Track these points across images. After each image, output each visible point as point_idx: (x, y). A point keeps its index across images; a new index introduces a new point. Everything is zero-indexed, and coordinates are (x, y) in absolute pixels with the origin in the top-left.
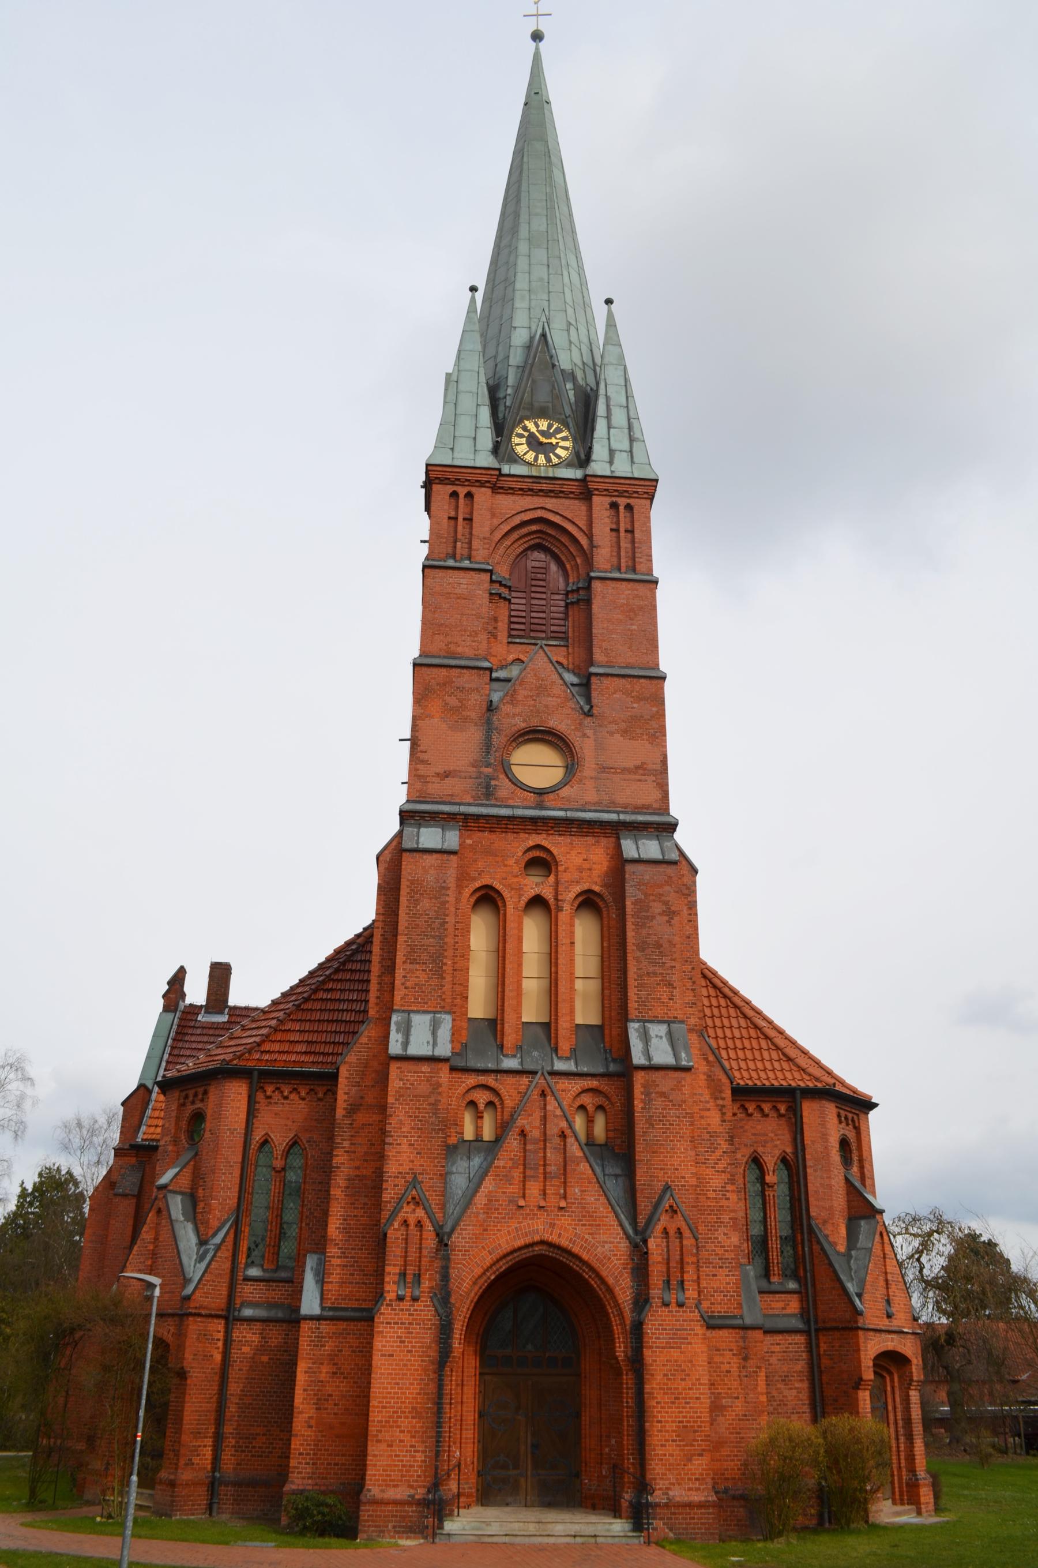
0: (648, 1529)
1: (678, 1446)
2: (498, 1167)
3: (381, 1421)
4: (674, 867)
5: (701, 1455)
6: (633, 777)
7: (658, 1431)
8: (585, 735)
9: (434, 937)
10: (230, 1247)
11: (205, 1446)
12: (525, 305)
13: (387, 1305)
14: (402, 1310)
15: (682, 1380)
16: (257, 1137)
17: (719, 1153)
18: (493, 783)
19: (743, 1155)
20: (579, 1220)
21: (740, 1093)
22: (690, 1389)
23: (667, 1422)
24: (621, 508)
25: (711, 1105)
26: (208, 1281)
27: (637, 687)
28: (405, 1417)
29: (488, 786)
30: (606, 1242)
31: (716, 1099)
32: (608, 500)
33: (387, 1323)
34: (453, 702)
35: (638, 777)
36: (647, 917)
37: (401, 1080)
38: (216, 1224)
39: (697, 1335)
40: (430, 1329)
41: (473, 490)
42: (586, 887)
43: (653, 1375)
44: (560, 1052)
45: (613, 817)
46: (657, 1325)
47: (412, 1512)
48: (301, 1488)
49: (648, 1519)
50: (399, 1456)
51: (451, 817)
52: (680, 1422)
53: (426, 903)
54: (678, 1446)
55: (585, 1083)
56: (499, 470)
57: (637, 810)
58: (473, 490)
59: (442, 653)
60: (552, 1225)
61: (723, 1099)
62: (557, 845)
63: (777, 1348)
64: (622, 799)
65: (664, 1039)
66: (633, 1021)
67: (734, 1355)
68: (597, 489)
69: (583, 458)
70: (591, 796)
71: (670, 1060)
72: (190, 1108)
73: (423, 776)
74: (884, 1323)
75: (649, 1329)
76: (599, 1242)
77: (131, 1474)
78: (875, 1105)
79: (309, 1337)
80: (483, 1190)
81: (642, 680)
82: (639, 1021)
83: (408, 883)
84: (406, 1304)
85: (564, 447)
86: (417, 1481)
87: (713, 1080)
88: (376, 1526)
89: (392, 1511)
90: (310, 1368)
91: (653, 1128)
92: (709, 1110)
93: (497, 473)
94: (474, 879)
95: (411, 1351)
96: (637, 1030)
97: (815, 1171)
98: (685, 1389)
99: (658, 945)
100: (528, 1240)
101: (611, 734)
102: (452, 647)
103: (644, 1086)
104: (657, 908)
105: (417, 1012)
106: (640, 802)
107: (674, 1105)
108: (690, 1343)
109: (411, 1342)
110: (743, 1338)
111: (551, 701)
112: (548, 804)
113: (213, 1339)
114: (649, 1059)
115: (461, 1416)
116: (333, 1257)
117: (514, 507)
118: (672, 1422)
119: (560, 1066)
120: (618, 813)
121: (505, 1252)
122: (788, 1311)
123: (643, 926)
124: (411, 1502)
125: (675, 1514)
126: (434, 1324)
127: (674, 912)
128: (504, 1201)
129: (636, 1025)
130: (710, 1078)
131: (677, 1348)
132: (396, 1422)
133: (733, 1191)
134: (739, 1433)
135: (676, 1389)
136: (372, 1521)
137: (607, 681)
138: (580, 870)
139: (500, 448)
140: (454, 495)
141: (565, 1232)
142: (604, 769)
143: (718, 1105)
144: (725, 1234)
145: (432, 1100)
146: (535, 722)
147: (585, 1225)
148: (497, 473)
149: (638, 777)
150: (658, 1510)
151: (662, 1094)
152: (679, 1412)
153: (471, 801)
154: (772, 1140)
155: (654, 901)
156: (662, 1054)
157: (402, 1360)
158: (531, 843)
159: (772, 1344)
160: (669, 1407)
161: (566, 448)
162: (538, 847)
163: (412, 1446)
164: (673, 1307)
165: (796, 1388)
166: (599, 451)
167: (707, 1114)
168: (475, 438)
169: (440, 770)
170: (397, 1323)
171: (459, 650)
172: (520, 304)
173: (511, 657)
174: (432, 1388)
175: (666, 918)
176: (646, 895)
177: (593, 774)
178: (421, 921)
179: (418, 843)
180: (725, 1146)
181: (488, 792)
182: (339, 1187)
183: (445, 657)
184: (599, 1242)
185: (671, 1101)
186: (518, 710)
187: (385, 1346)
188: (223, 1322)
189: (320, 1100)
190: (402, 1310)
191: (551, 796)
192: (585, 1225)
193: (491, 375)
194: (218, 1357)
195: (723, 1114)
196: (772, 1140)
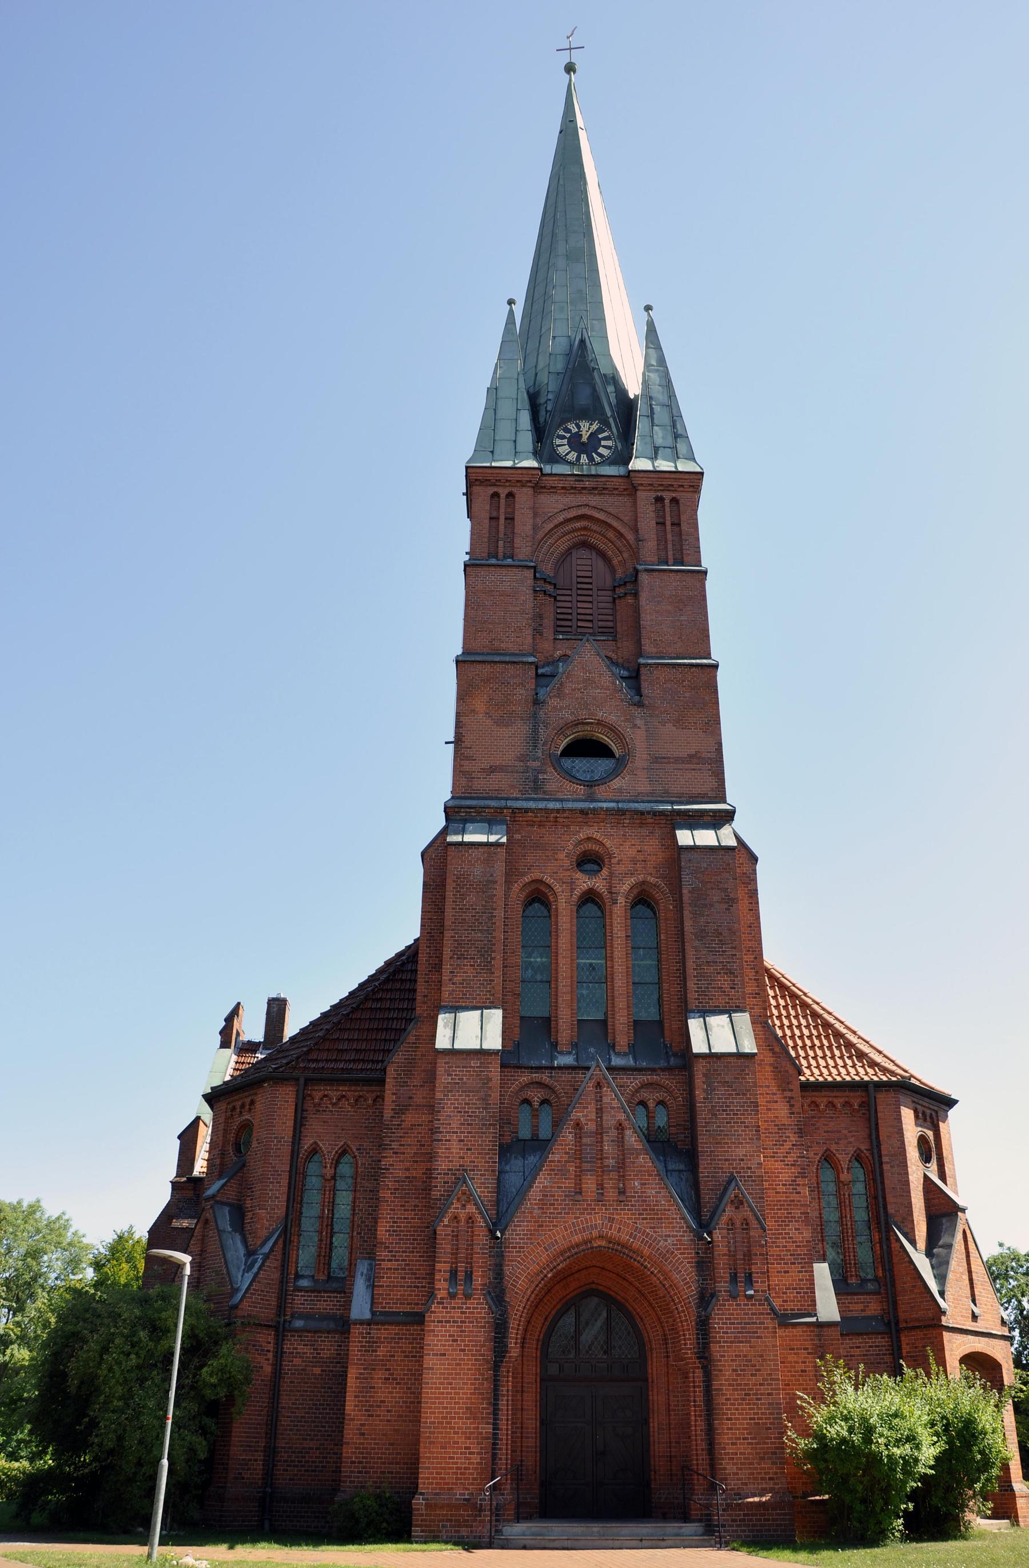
1: (749, 1444)
2: (553, 1161)
3: (434, 1423)
7: (728, 1429)
8: (635, 726)
10: (279, 1257)
11: (256, 1460)
13: (438, 1303)
14: (454, 1308)
15: (752, 1375)
17: (788, 1145)
19: (815, 1154)
22: (761, 1384)
23: (738, 1419)
24: (667, 502)
28: (461, 1418)
29: (536, 780)
30: (669, 1236)
31: (784, 1090)
32: (654, 495)
33: (438, 1322)
38: (264, 1233)
39: (767, 1328)
40: (484, 1327)
41: (514, 490)
43: (721, 1370)
46: (725, 1318)
50: (453, 1458)
52: (751, 1419)
53: (472, 898)
54: (749, 1444)
56: (541, 469)
61: (791, 1090)
67: (809, 1353)
70: (643, 787)
74: (970, 1325)
76: (661, 1236)
78: (955, 1102)
79: (359, 1342)
90: (361, 1374)
91: (717, 1118)
94: (523, 874)
95: (464, 1350)
97: (892, 1167)
101: (663, 723)
102: (496, 643)
109: (464, 1341)
110: (818, 1336)
113: (263, 1350)
116: (384, 1260)
118: (743, 1419)
119: (616, 1061)
122: (868, 1313)
126: (488, 1322)
131: (746, 1342)
135: (745, 1385)
140: (495, 495)
142: (656, 760)
143: (785, 1098)
144: (796, 1229)
147: (646, 1219)
159: (851, 1348)
168: (515, 441)
169: (485, 765)
170: (449, 1322)
175: (726, 906)
180: (793, 1138)
182: (389, 1189)
184: (661, 1236)
190: (454, 1308)
192: (646, 1219)
194: (268, 1369)
195: (792, 1106)
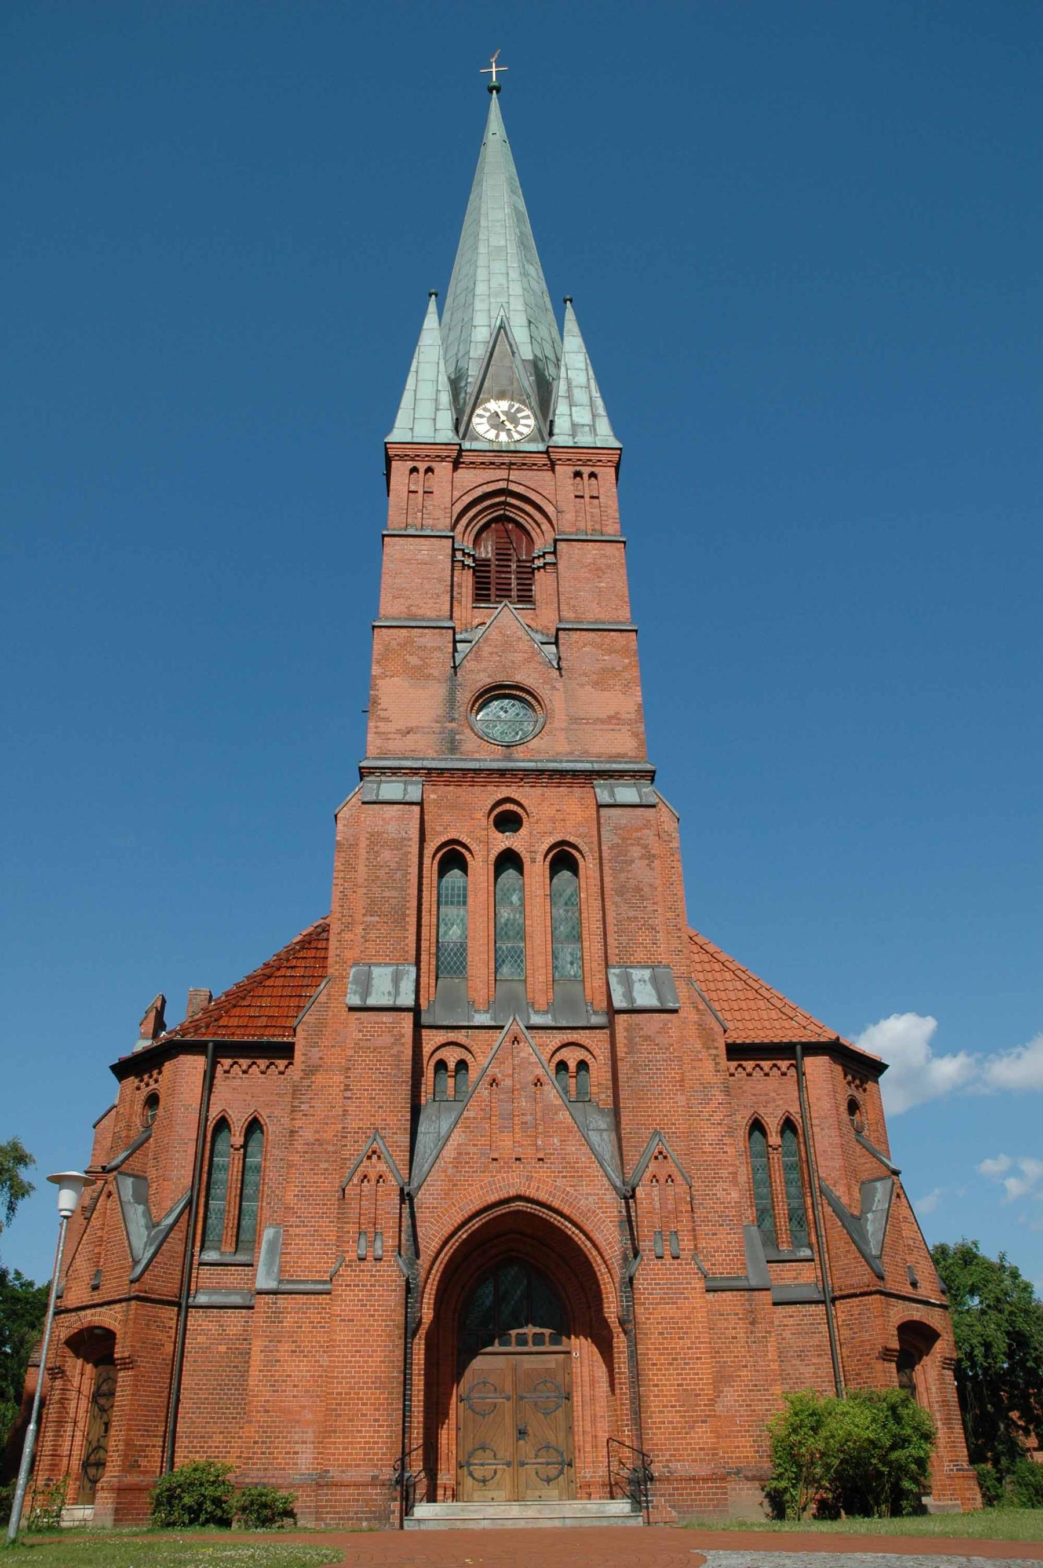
0: (647, 1508)
1: (677, 1412)
2: (468, 1118)
3: (341, 1394)
4: (654, 810)
5: (705, 1422)
6: (606, 727)
7: (655, 1396)
8: (554, 688)
9: (395, 888)
10: (184, 1229)
11: (154, 1446)
12: (485, 306)
13: (346, 1266)
14: (363, 1271)
15: (679, 1338)
16: (214, 1114)
17: (714, 1104)
18: (457, 737)
19: (742, 1120)
20: (559, 1172)
21: (737, 1052)
22: (688, 1348)
23: (665, 1385)
24: (585, 476)
25: (704, 1054)
26: (159, 1263)
27: (607, 641)
28: (369, 1388)
29: (452, 741)
30: (590, 1194)
31: (708, 1048)
32: (573, 469)
33: (346, 1286)
34: (414, 660)
35: (611, 727)
36: (626, 862)
37: (360, 1031)
38: (169, 1204)
39: (695, 1289)
40: (395, 1291)
41: (434, 465)
42: (558, 838)
43: (646, 1334)
44: (536, 1006)
45: (588, 766)
46: (650, 1276)
47: (376, 1494)
48: (255, 1481)
49: (646, 1496)
50: (361, 1431)
51: (414, 771)
52: (678, 1385)
53: (386, 855)
54: (677, 1412)
55: (565, 1037)
56: (460, 445)
57: (612, 758)
58: (434, 465)
59: (403, 615)
60: (529, 1178)
61: (716, 1048)
62: (527, 795)
63: (791, 1321)
64: (595, 749)
65: (648, 983)
66: (614, 967)
67: (739, 1319)
68: (560, 460)
69: (547, 427)
70: (562, 746)
71: (653, 1002)
72: (145, 1092)
73: (384, 733)
74: (907, 1290)
75: (639, 1283)
76: (582, 1195)
77: (29, 1422)
78: (886, 1067)
79: (265, 1312)
80: (453, 1142)
81: (613, 633)
82: (620, 967)
83: (368, 835)
84: (368, 1265)
85: (527, 424)
86: (382, 1460)
87: (704, 1029)
88: (335, 1513)
89: (352, 1494)
90: (266, 1347)
91: (639, 1073)
92: (701, 1060)
93: (458, 447)
94: (440, 833)
95: (373, 1316)
96: (617, 976)
97: (822, 1129)
98: (683, 1349)
99: (638, 889)
100: (503, 1194)
101: (582, 686)
102: (414, 609)
103: (627, 1030)
104: (636, 852)
105: (379, 965)
106: (614, 751)
107: (660, 1049)
108: (688, 1298)
109: (373, 1305)
110: (748, 1300)
111: (518, 657)
112: (516, 756)
113: (164, 1327)
114: (632, 1000)
115: (438, 1398)
116: (291, 1226)
117: (473, 481)
118: (671, 1385)
119: (536, 1020)
120: (592, 762)
121: (478, 1208)
122: (801, 1281)
123: (622, 870)
124: (374, 1482)
125: (677, 1489)
126: (399, 1286)
127: (654, 856)
128: (474, 1154)
129: (617, 971)
130: (701, 1026)
131: (673, 1303)
132: (357, 1394)
133: (731, 1144)
134: (750, 1405)
135: (672, 1349)
136: (332, 1507)
137: (575, 635)
138: (553, 820)
139: (461, 424)
140: (414, 470)
141: (544, 1186)
142: (574, 720)
143: (710, 1055)
144: (724, 1190)
145: (394, 1051)
146: (501, 678)
147: (565, 1177)
148: (458, 447)
149: (611, 727)
150: (658, 1485)
151: (647, 1038)
152: (678, 1374)
153: (435, 755)
154: (774, 1100)
155: (632, 845)
156: (645, 996)
157: (364, 1326)
158: (500, 796)
159: (784, 1317)
160: (666, 1369)
161: (528, 426)
162: (508, 800)
163: (375, 1420)
164: (668, 1261)
165: (814, 1364)
166: (562, 424)
167: (699, 1064)
168: (435, 420)
169: (401, 725)
170: (358, 1286)
171: (420, 612)
172: (479, 305)
173: (476, 622)
174: (399, 1353)
175: (647, 862)
176: (623, 839)
177: (564, 725)
178: (381, 873)
179: (377, 795)
180: (721, 1097)
181: (453, 746)
182: (297, 1152)
183: (406, 619)
184: (582, 1195)
185: (658, 1045)
186: (483, 665)
187: (344, 1310)
188: (176, 1309)
189: (281, 1073)
190: (363, 1271)
191: (520, 748)
192: (565, 1177)
193: (452, 369)
194: (169, 1348)
195: (717, 1064)
196: (774, 1100)
